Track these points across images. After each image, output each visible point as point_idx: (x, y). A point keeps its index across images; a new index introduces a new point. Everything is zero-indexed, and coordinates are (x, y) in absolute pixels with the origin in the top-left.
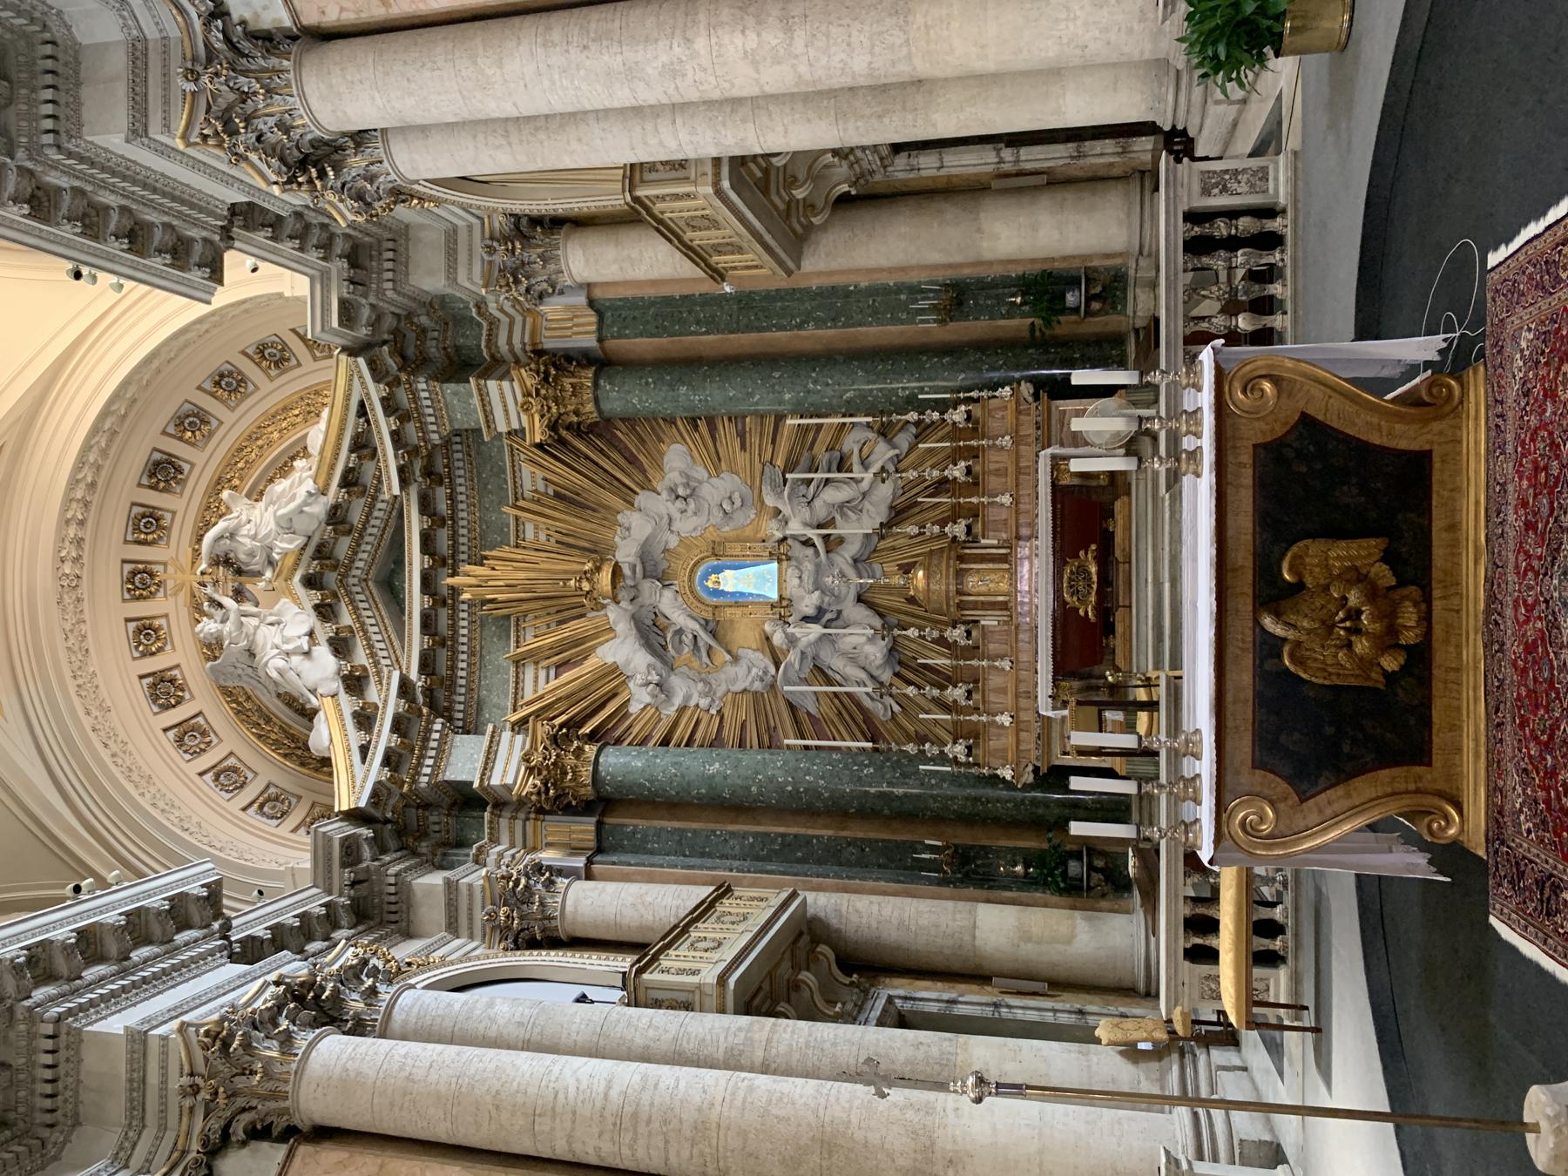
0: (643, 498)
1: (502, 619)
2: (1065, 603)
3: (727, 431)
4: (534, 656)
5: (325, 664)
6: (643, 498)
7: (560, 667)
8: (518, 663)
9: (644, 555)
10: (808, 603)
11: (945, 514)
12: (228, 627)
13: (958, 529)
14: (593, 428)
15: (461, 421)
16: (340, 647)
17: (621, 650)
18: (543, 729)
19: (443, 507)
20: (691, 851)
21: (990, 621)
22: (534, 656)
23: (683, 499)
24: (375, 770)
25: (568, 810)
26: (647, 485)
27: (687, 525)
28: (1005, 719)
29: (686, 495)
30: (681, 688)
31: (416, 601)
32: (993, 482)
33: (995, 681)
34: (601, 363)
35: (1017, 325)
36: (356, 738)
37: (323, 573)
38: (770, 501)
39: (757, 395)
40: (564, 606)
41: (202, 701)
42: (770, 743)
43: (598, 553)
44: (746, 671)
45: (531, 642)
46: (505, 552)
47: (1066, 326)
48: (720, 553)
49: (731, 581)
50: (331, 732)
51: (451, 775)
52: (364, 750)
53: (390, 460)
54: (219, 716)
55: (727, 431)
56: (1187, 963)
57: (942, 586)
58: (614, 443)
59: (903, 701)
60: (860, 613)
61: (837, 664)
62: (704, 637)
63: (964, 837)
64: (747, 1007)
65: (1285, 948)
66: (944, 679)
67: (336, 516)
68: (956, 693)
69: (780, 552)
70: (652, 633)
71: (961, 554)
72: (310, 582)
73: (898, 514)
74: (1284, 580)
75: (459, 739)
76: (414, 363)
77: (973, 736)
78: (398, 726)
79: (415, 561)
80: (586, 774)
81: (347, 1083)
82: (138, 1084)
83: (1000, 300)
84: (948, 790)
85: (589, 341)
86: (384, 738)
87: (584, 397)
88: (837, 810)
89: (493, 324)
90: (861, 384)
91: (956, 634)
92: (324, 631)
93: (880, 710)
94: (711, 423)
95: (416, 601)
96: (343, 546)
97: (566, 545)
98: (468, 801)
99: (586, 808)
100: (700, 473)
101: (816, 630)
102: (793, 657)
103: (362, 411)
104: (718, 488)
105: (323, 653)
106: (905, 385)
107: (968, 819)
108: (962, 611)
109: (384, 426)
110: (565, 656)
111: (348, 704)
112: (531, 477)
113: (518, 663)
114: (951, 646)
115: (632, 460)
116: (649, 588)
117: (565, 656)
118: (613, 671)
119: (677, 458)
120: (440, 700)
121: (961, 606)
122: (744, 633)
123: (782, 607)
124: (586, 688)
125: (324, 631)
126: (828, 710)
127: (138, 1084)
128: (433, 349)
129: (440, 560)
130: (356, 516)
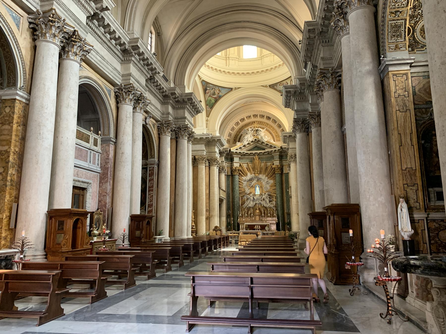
0: (267, 178)
1: (252, 161)
3: (275, 188)
4: (248, 165)
5: (246, 143)
6: (267, 178)
7: (247, 168)
8: (247, 163)
9: (260, 178)
10: (255, 198)
11: (264, 212)
12: (250, 132)
13: (263, 215)
14: (274, 172)
15: (275, 157)
16: (248, 144)
17: (249, 176)
18: (240, 169)
19: (265, 154)
20: (228, 186)
21: (254, 218)
22: (248, 165)
23: (267, 182)
24: (235, 151)
25: (231, 172)
26: (268, 178)
27: (264, 183)
29: (267, 183)
30: (245, 183)
31: (254, 152)
34: (282, 174)
36: (238, 148)
37: (257, 141)
38: (267, 193)
39: (278, 192)
40: (254, 169)
41: (241, 124)
42: (240, 193)
43: (260, 173)
44: (248, 191)
45: (250, 165)
46: (260, 162)
48: (261, 187)
49: (258, 189)
50: (239, 144)
51: (235, 158)
52: (237, 149)
54: (240, 126)
55: (275, 188)
57: (257, 214)
58: (273, 174)
59: (245, 209)
60: (254, 203)
61: (249, 201)
63: (231, 215)
64: (219, 199)
66: (247, 214)
67: (263, 142)
68: (246, 215)
69: (261, 195)
70: (251, 180)
72: (255, 140)
73: (266, 207)
76: (281, 152)
77: (242, 217)
78: (240, 153)
79: (258, 152)
80: (235, 174)
81: (214, 171)
82: (212, 152)
85: (284, 172)
86: (238, 151)
87: (278, 172)
88: (233, 202)
89: (286, 161)
90: (279, 203)
91: (252, 215)
92: (250, 142)
93: (244, 206)
94: (275, 186)
95: (254, 152)
96: (260, 143)
97: (261, 168)
98: (232, 160)
99: (232, 173)
100: (270, 184)
102: (249, 196)
104: (268, 186)
105: (248, 142)
106: (279, 209)
108: (255, 215)
109: (273, 150)
110: (248, 169)
111: (242, 146)
112: (269, 164)
113: (247, 163)
114: (251, 214)
115: (271, 176)
116: (257, 179)
117: (248, 169)
118: (247, 175)
119: (271, 182)
120: (242, 156)
122: (252, 190)
123: (255, 195)
124: (244, 172)
126: (244, 200)
128: (283, 154)
129: (259, 154)
130: (263, 144)
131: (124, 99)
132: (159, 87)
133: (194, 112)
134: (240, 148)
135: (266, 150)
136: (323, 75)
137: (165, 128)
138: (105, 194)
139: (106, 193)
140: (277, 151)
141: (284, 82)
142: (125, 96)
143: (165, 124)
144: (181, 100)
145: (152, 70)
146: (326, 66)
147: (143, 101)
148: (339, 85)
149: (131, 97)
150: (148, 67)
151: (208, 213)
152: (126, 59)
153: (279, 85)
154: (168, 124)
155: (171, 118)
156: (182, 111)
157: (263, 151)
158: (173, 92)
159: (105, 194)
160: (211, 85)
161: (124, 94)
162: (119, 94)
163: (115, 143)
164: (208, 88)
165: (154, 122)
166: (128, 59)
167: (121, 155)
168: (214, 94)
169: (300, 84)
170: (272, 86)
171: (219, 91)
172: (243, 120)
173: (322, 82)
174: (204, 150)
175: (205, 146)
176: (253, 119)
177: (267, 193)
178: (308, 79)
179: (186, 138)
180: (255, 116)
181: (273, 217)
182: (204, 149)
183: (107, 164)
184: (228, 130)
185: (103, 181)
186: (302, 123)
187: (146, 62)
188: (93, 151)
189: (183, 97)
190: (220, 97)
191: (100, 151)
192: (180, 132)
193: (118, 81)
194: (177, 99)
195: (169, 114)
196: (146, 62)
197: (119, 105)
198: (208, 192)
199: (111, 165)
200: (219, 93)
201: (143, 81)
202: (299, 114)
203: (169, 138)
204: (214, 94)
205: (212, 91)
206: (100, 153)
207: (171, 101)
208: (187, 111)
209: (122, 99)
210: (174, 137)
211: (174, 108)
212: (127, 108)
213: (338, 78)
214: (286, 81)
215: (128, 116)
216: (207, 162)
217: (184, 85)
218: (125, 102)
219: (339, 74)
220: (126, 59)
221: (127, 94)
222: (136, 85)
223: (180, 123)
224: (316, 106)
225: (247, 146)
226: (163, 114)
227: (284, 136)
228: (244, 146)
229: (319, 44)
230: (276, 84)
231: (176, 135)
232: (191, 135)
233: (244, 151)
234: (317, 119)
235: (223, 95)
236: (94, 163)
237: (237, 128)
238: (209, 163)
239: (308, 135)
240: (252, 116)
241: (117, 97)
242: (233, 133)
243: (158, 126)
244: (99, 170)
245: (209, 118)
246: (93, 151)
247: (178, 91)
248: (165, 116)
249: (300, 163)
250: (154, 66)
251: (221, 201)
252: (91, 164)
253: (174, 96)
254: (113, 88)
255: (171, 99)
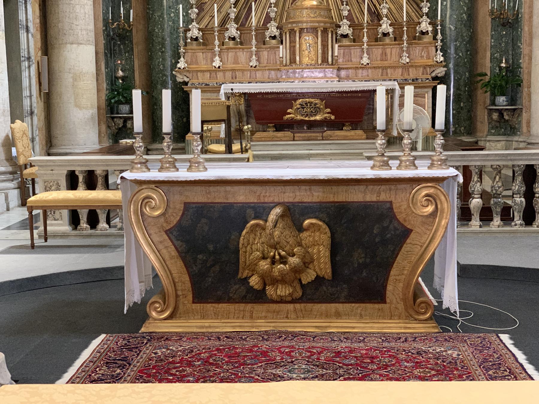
2: (295, 100)
13: (345, 29)
21: (282, 51)
28: (217, 63)
32: (377, 51)
33: (242, 56)
35: (486, 65)
47: (483, 97)
56: (65, 172)
63: (138, 37)
65: (82, 229)
66: (242, 21)
68: (233, 30)
71: (328, 31)
74: (304, 221)
77: (205, 41)
83: (505, 52)
84: (168, 25)
91: (273, 29)
107: (150, 40)
108: (289, 33)
121: (292, 32)
181: (416, 37)
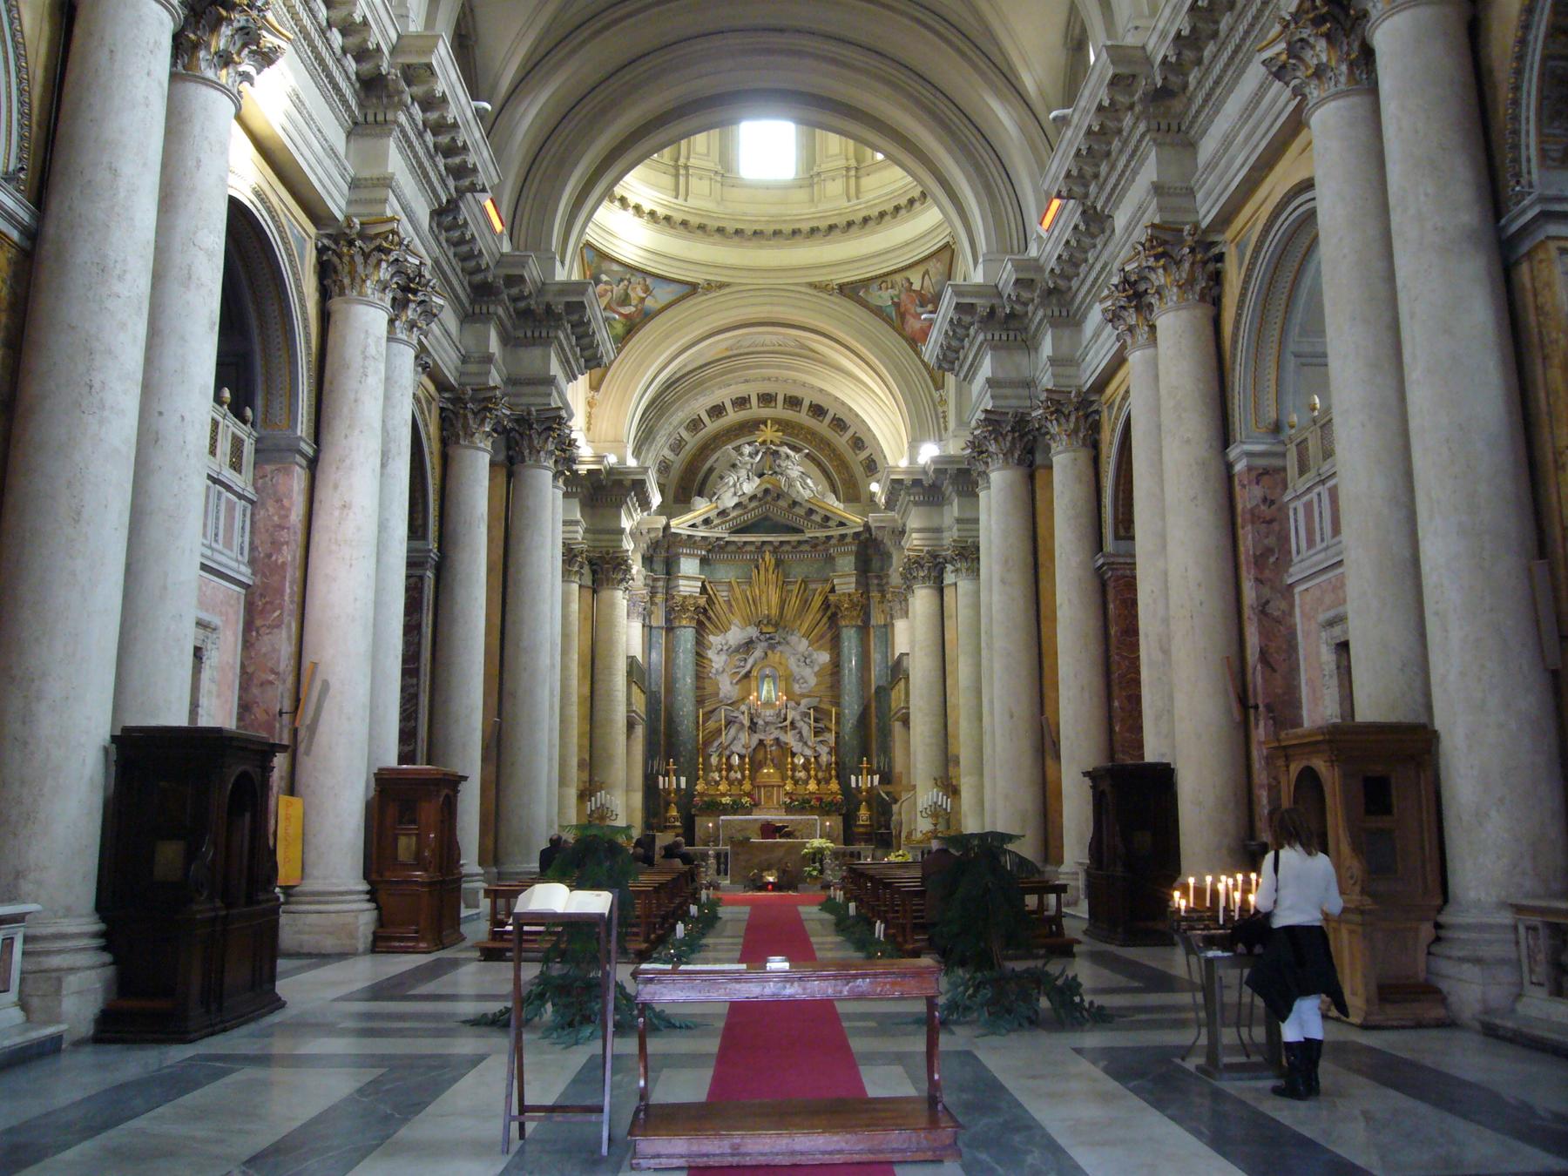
5: (729, 501)
16: (738, 505)
37: (768, 495)
41: (712, 426)
50: (702, 507)
51: (683, 560)
52: (693, 526)
53: (821, 534)
60: (754, 742)
61: (733, 731)
62: (744, 672)
67: (795, 503)
72: (766, 491)
75: (697, 561)
85: (873, 622)
86: (701, 533)
92: (745, 500)
99: (668, 620)
100: (816, 669)
101: (747, 723)
103: (842, 524)
109: (836, 532)
111: (713, 514)
115: (822, 637)
120: (712, 553)
125: (745, 500)
127: (609, 532)
129: (776, 549)
131: (357, 281)
132: (465, 248)
133: (577, 360)
134: (707, 522)
135: (809, 535)
136: (1160, 250)
137: (470, 416)
138: (272, 677)
139: (273, 671)
140: (849, 540)
141: (898, 278)
142: (360, 268)
143: (473, 400)
144: (541, 309)
145: (460, 172)
146: (1170, 217)
147: (420, 297)
148: (1215, 292)
149: (384, 273)
150: (450, 161)
151: (585, 776)
152: (371, 118)
153: (876, 286)
154: (485, 402)
155: (495, 379)
156: (537, 352)
157: (794, 538)
158: (516, 272)
159: (272, 677)
160: (615, 267)
161: (359, 259)
162: (335, 260)
163: (313, 464)
164: (604, 278)
165: (432, 388)
166: (380, 118)
167: (337, 513)
168: (625, 300)
169: (1017, 281)
170: (850, 291)
171: (647, 290)
172: (717, 411)
173: (1153, 276)
174: (576, 523)
175: (583, 506)
176: (755, 411)
177: (804, 702)
178: (1053, 263)
179: (551, 463)
180: (767, 399)
182: (579, 516)
183: (279, 551)
184: (661, 448)
185: (259, 623)
186: (1013, 430)
187: (444, 139)
188: (228, 488)
189: (549, 298)
190: (647, 316)
191: (250, 492)
192: (530, 434)
193: (337, 204)
194: (522, 305)
195: (488, 359)
196: (444, 139)
197: (336, 304)
198: (587, 691)
199: (289, 555)
200: (642, 300)
201: (423, 214)
202: (1006, 397)
203: (484, 459)
204: (625, 300)
205: (618, 290)
206: (252, 502)
207: (500, 311)
208: (558, 355)
209: (347, 281)
210: (501, 457)
211: (506, 340)
212: (368, 319)
213: (1211, 267)
214: (907, 274)
215: (372, 351)
216: (586, 570)
217: (548, 249)
218: (360, 294)
219: (1216, 250)
220: (371, 118)
221: (373, 260)
222: (405, 230)
223: (531, 401)
224: (1070, 371)
225: (733, 514)
226: (465, 360)
227: (894, 481)
228: (723, 513)
229: (1143, 136)
230: (866, 283)
231: (509, 448)
232: (566, 451)
233: (719, 532)
234: (1073, 418)
235: (658, 306)
236: (228, 544)
237: (692, 441)
238: (594, 572)
239: (1031, 478)
240: (754, 400)
241: (325, 270)
242: (678, 462)
243: (442, 409)
244: (244, 573)
245: (598, 396)
246: (228, 488)
247: (533, 272)
248: (472, 368)
249: (1003, 581)
250: (471, 159)
251: (630, 726)
252: (220, 547)
253: (515, 291)
254: (312, 230)
255: (501, 302)
